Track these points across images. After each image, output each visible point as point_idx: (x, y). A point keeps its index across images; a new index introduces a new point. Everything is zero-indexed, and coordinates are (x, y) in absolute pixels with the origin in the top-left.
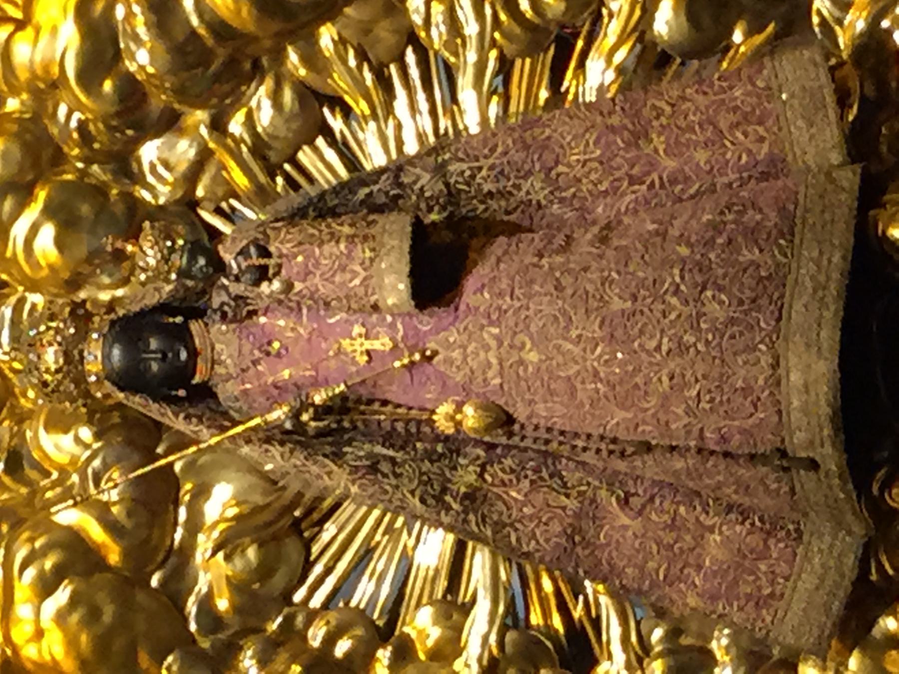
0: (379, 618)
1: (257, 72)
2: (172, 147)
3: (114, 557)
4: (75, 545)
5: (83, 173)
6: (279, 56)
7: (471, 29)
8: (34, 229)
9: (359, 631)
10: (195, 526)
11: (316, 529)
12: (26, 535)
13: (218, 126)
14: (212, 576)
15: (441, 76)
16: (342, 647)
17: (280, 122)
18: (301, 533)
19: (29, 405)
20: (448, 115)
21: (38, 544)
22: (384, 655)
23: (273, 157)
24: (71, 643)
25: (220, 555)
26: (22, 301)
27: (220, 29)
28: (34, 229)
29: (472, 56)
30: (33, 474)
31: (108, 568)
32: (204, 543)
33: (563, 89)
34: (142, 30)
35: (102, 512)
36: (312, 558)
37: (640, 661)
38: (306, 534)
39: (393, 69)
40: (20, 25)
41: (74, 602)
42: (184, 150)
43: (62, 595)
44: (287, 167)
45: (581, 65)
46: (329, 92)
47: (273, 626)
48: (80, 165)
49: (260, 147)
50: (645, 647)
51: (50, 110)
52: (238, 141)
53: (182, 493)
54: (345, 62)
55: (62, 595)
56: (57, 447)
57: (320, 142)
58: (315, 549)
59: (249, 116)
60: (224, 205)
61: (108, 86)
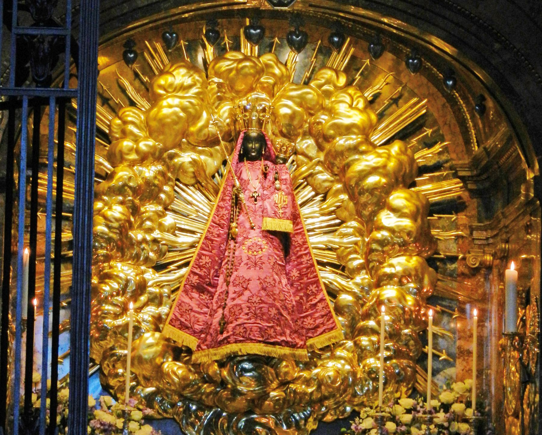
1: (334, 174)
3: (193, 129)
4: (196, 117)
5: (306, 121)
6: (339, 181)
7: (345, 240)
9: (168, 202)
10: (200, 153)
13: (319, 163)
14: (186, 158)
15: (331, 230)
16: (163, 196)
17: (319, 181)
18: (196, 183)
22: (160, 208)
23: (309, 179)
24: (167, 116)
27: (348, 165)
29: (337, 240)
30: (216, 104)
31: (188, 126)
32: (195, 156)
35: (206, 126)
37: (158, 286)
38: (196, 186)
39: (334, 216)
40: (351, 106)
41: (179, 118)
42: (313, 152)
43: (182, 114)
44: (306, 183)
45: (334, 272)
46: (327, 197)
47: (169, 175)
50: (162, 287)
52: (314, 169)
54: (336, 202)
55: (182, 114)
57: (313, 193)
58: (191, 188)
61: (332, 132)
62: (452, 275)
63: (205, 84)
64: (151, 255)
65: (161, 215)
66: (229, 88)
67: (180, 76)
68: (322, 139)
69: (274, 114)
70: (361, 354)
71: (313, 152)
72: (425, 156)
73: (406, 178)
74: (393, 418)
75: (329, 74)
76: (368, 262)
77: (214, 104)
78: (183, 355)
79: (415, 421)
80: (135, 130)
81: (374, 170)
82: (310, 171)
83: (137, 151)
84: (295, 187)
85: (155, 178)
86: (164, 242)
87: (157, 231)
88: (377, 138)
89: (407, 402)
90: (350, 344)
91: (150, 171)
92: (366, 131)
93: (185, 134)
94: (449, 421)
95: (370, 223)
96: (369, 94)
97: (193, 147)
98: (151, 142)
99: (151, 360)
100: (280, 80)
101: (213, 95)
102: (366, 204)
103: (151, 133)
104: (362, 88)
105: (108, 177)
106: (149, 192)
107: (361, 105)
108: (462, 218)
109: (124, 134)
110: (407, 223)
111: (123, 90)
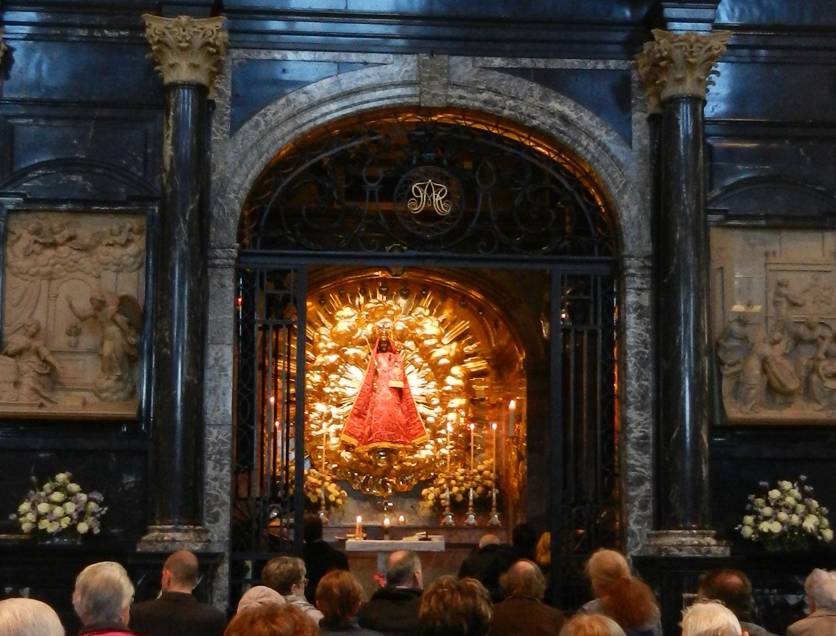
3: (354, 337)
14: (350, 351)
22: (338, 376)
35: (360, 336)
42: (413, 348)
49: (413, 359)
62: (484, 408)
63: (359, 315)
64: (334, 399)
65: (338, 380)
66: (372, 316)
67: (347, 311)
68: (418, 341)
69: (394, 330)
70: (438, 447)
71: (413, 348)
72: (469, 349)
73: (458, 360)
74: (454, 478)
75: (420, 309)
76: (441, 401)
79: (466, 480)
80: (326, 338)
81: (443, 357)
83: (327, 348)
84: (404, 365)
88: (445, 341)
89: (461, 470)
90: (432, 442)
91: (333, 358)
92: (440, 337)
93: (350, 339)
94: (482, 479)
95: (441, 383)
96: (441, 319)
97: (354, 346)
98: (333, 344)
99: (335, 452)
100: (397, 313)
102: (439, 373)
103: (334, 339)
104: (437, 316)
105: (313, 361)
106: (332, 368)
107: (437, 324)
108: (488, 379)
109: (320, 340)
110: (460, 382)
111: (319, 318)
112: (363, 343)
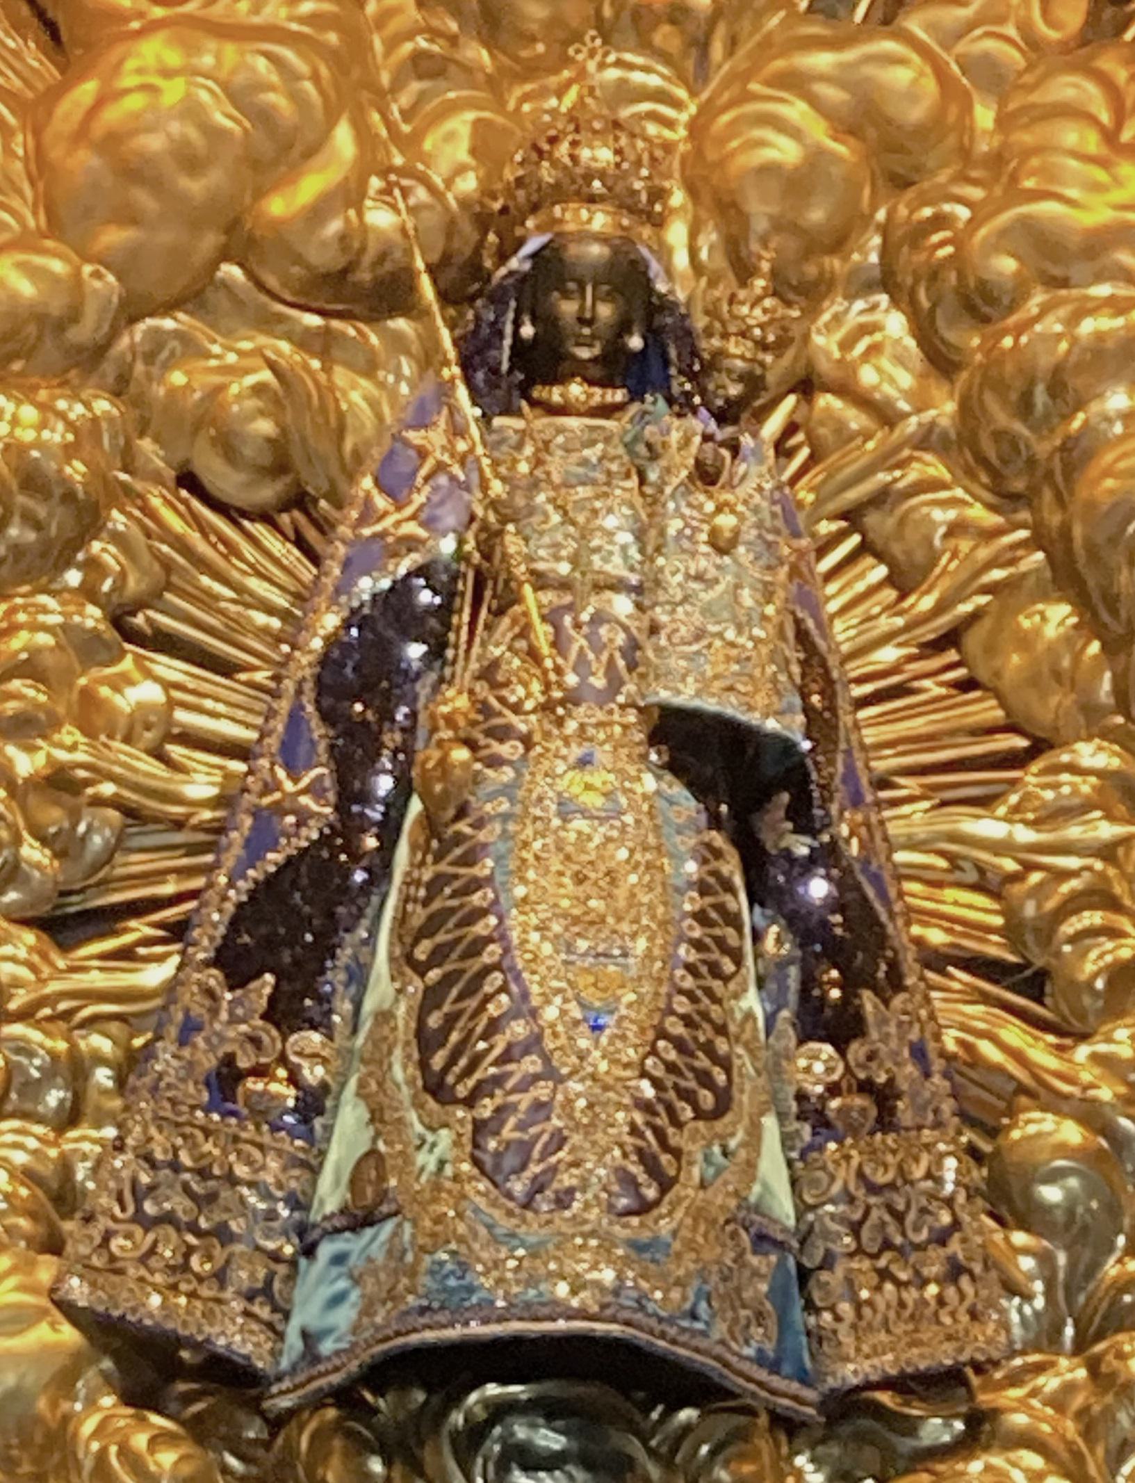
0: (149, 620)
2: (900, 360)
8: (795, 133)
11: (292, 536)
12: (324, 71)
18: (285, 508)
19: (511, 105)
20: (917, 792)
21: (308, 86)
25: (266, 376)
26: (677, 104)
28: (795, 133)
31: (260, 193)
33: (951, 969)
34: (1088, 326)
36: (246, 523)
38: (285, 519)
44: (855, 539)
48: (881, 215)
51: (975, 174)
53: (361, 325)
56: (451, 137)
58: (258, 529)
59: (936, 485)
60: (800, 437)
61: (1007, 265)
68: (952, 307)
77: (397, 85)
78: (182, 1387)
82: (883, 477)
85: (70, 451)
86: (108, 789)
87: (69, 734)
101: (392, 44)
112: (362, 290)
